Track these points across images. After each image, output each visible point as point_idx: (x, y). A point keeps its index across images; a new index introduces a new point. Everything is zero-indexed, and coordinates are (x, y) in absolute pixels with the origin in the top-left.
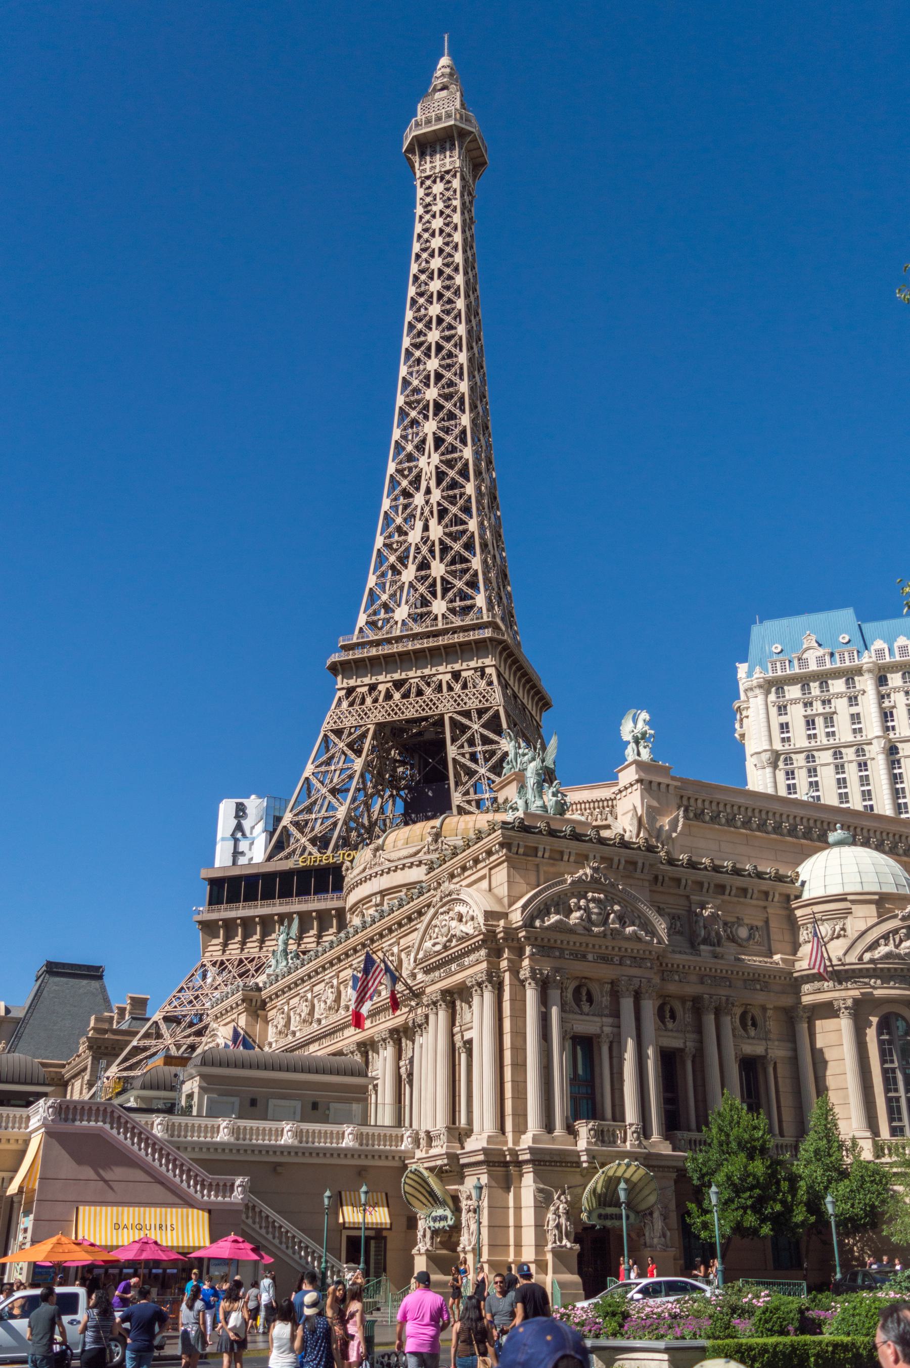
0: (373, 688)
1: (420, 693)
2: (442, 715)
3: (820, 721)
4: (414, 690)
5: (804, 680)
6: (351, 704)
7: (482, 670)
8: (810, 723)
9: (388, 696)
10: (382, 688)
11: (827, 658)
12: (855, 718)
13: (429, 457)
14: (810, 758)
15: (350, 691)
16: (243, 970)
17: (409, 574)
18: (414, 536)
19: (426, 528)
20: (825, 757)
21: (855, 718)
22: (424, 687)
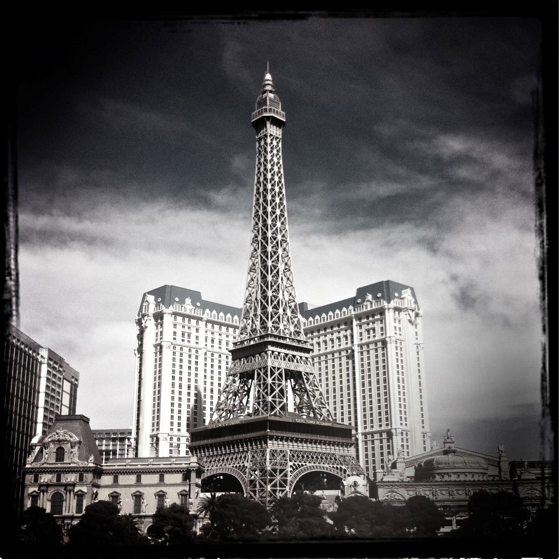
0: (279, 353)
1: (293, 361)
2: (300, 373)
3: (186, 335)
4: (291, 359)
5: (184, 316)
7: (307, 358)
8: (183, 335)
9: (284, 359)
11: (193, 310)
12: (197, 337)
14: (181, 349)
15: (273, 352)
17: (281, 311)
19: (283, 295)
20: (186, 350)
21: (197, 337)
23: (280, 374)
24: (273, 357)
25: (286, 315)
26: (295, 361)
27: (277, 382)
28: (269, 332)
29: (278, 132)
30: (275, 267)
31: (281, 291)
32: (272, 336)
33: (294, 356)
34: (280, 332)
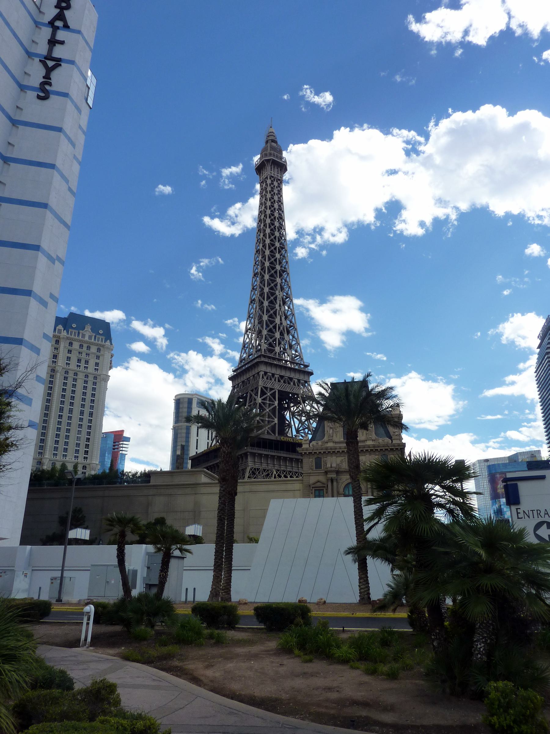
0: (273, 375)
1: (289, 384)
6: (267, 379)
9: (279, 381)
15: (266, 373)
16: (267, 473)
17: (277, 335)
18: (277, 321)
19: (281, 320)
23: (273, 395)
24: (265, 378)
25: (283, 339)
26: (292, 383)
28: (263, 353)
29: (279, 175)
30: (273, 294)
31: (278, 317)
32: (264, 356)
33: (291, 379)
34: (276, 353)
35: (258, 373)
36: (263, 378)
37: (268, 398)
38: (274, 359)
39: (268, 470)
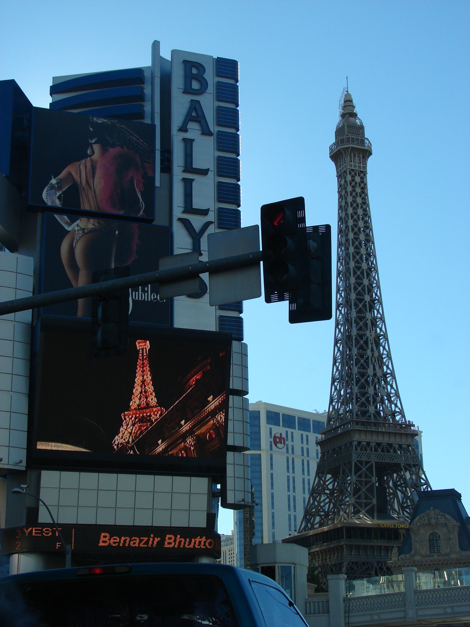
1: (388, 451)
4: (385, 449)
6: (361, 450)
9: (376, 450)
10: (373, 445)
13: (370, 332)
15: (359, 443)
16: (366, 567)
19: (374, 369)
22: (389, 449)
23: (370, 469)
24: (359, 448)
26: (392, 451)
27: (364, 479)
29: (362, 165)
31: (371, 366)
33: (390, 445)
34: (370, 416)
35: (351, 443)
36: (356, 449)
37: (364, 473)
38: (369, 424)
39: (368, 563)
